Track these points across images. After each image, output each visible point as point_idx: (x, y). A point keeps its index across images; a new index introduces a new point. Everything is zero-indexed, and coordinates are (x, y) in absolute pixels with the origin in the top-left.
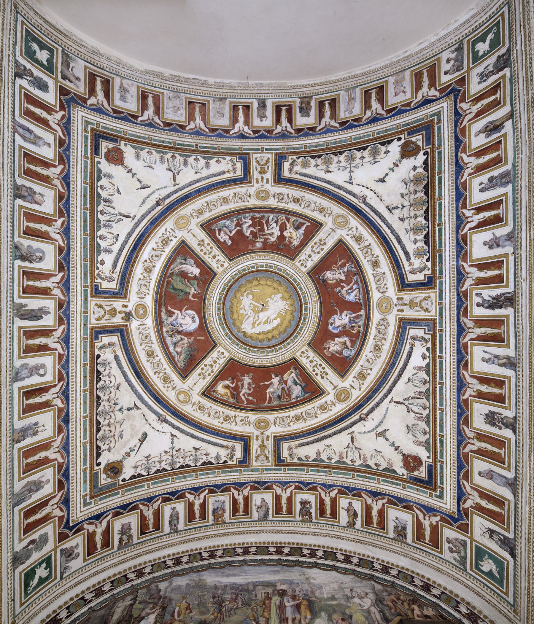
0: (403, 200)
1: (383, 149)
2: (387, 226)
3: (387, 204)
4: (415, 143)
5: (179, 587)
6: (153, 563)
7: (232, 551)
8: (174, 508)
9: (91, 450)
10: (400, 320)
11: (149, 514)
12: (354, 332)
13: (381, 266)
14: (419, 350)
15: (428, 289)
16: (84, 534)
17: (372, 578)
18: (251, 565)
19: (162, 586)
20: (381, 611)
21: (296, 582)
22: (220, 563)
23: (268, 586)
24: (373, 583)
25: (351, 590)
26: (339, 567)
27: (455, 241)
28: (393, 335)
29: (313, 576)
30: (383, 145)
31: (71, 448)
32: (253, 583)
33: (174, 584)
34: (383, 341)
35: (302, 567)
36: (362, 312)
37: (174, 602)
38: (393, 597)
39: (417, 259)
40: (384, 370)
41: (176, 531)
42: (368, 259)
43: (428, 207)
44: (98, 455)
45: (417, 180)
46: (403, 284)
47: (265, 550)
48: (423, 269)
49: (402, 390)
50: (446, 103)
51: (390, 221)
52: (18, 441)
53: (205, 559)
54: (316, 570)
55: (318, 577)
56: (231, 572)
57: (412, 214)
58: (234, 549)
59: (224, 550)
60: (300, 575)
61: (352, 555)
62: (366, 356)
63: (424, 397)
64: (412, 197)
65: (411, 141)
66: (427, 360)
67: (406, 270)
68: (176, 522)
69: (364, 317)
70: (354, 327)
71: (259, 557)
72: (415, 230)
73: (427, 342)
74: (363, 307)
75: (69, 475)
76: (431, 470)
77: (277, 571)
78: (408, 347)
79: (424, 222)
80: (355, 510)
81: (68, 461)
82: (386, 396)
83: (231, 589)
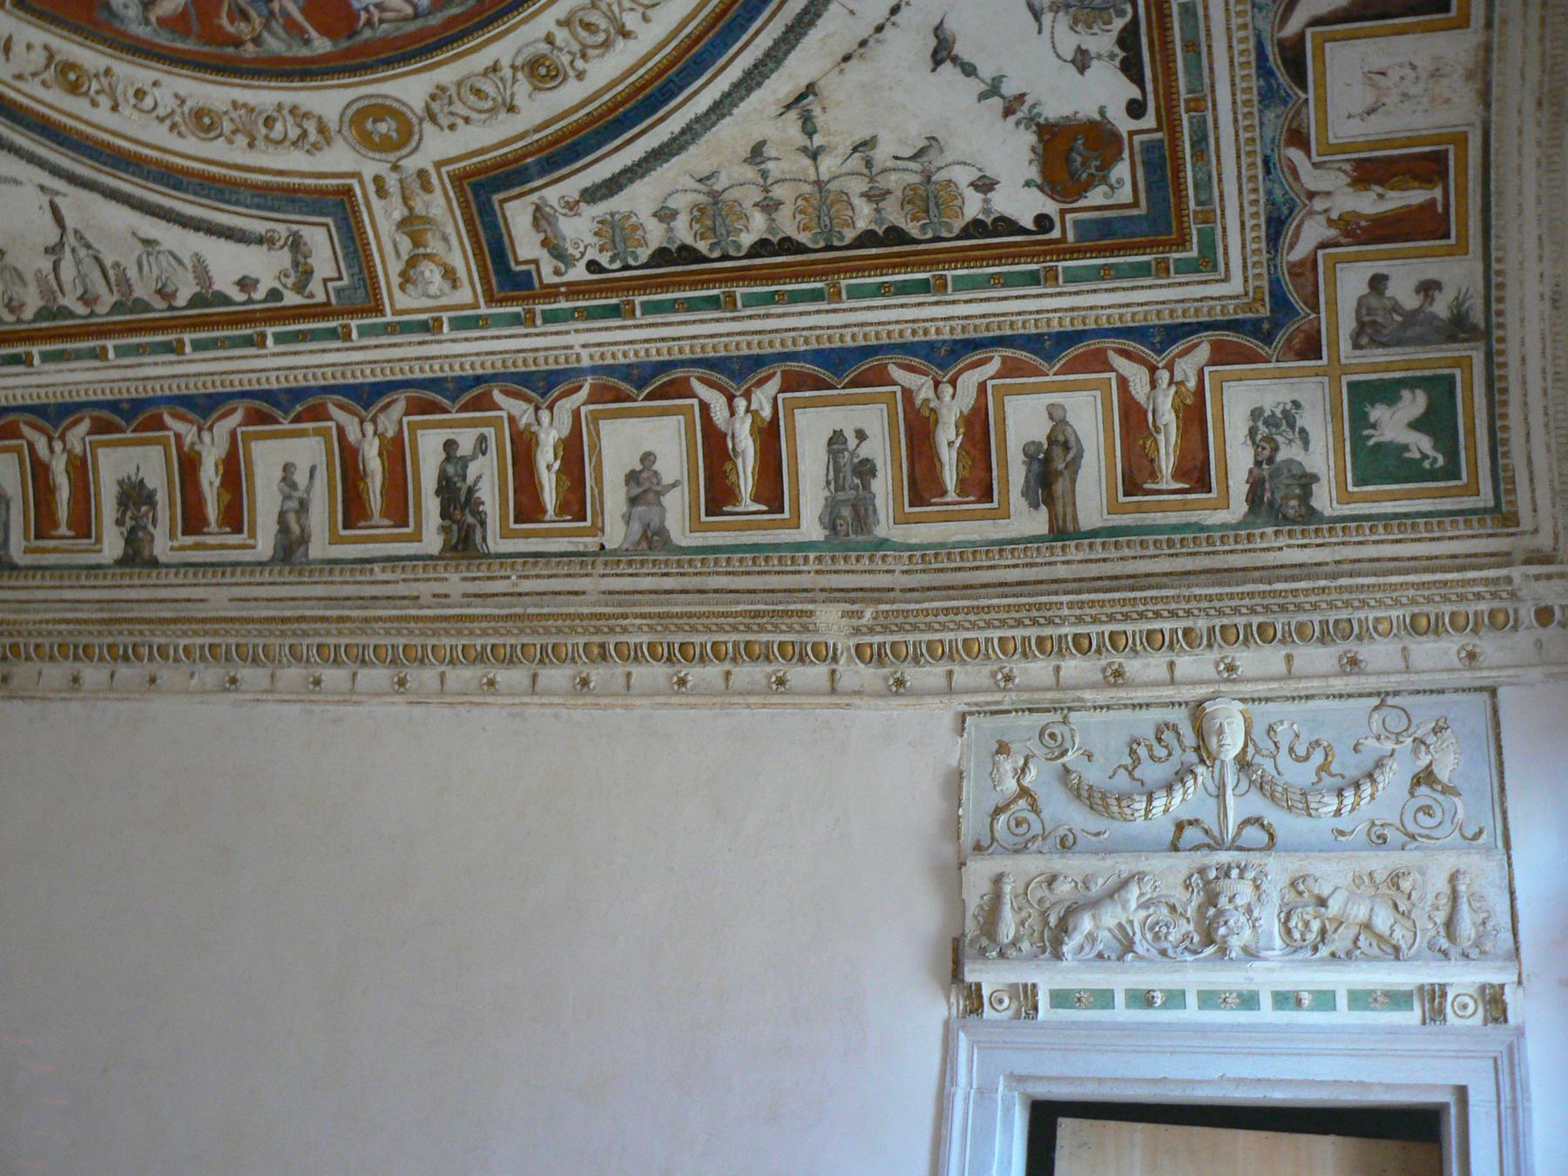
0: (844, 147)
1: (1103, 41)
2: (726, 95)
3: (826, 88)
4: (1101, 175)
10: (349, 191)
12: (225, 21)
13: (541, 96)
14: (267, 267)
15: (485, 279)
27: (665, 357)
28: (281, 173)
30: (1121, 42)
34: (242, 140)
36: (322, 45)
39: (596, 226)
40: (138, 156)
42: (561, 36)
43: (808, 250)
45: (929, 197)
46: (484, 187)
48: (558, 253)
49: (111, 224)
50: (1241, 290)
51: (744, 107)
57: (778, 192)
62: (155, 84)
63: (116, 297)
64: (857, 186)
65: (1118, 157)
66: (239, 297)
67: (544, 192)
69: (305, 52)
70: (246, 17)
72: (714, 210)
73: (300, 288)
74: (344, 44)
78: (259, 227)
79: (747, 240)
82: (55, 171)
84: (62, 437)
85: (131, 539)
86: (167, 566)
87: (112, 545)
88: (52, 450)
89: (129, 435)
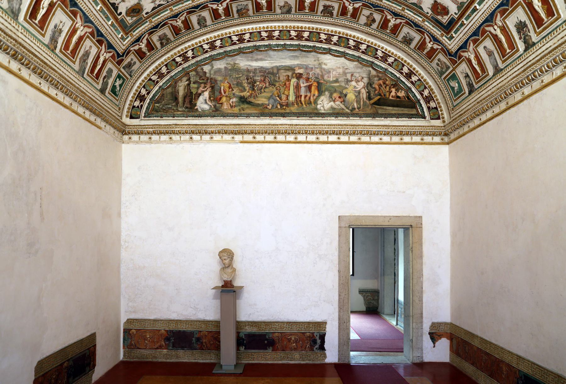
5: (219, 71)
6: (192, 48)
7: (258, 35)
8: (200, 16)
9: (109, 9)
11: (179, 23)
16: (133, 53)
17: (372, 65)
18: (275, 50)
19: (206, 68)
20: (369, 92)
21: (310, 66)
22: (249, 48)
23: (288, 70)
24: (371, 69)
25: (352, 75)
26: (348, 54)
29: (325, 61)
31: (91, 18)
32: (277, 67)
33: (215, 67)
35: (318, 52)
37: (219, 82)
38: (381, 82)
41: (206, 26)
44: (116, 9)
47: (287, 34)
52: (55, 47)
53: (235, 44)
54: (328, 57)
55: (331, 63)
56: (259, 57)
58: (260, 32)
59: (251, 33)
60: (315, 61)
61: (362, 42)
68: (204, 22)
71: (282, 42)
75: (102, 33)
76: (452, 23)
77: (296, 56)
80: (374, 18)
81: (96, 27)
83: (260, 72)
84: (496, 24)
85: (525, 42)
86: (538, 42)
87: (521, 46)
88: (495, 30)
89: (510, 9)
